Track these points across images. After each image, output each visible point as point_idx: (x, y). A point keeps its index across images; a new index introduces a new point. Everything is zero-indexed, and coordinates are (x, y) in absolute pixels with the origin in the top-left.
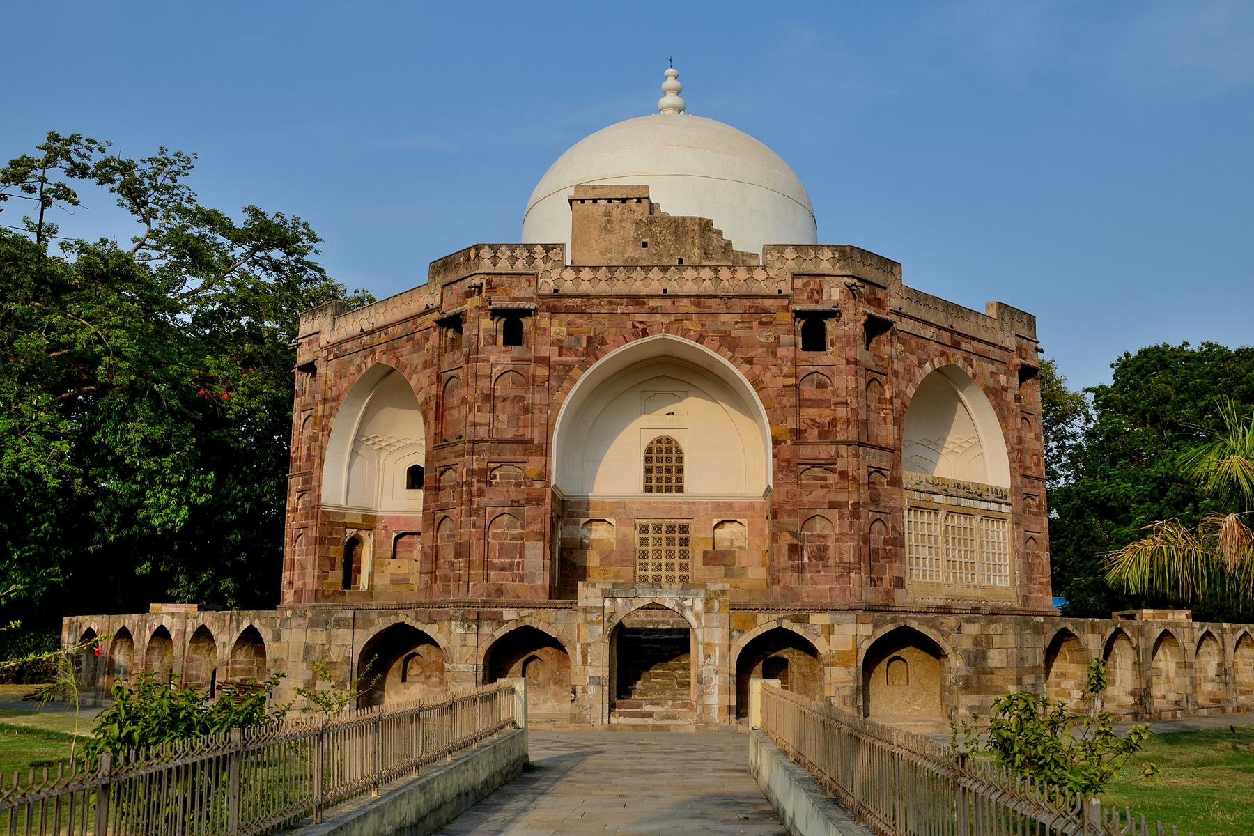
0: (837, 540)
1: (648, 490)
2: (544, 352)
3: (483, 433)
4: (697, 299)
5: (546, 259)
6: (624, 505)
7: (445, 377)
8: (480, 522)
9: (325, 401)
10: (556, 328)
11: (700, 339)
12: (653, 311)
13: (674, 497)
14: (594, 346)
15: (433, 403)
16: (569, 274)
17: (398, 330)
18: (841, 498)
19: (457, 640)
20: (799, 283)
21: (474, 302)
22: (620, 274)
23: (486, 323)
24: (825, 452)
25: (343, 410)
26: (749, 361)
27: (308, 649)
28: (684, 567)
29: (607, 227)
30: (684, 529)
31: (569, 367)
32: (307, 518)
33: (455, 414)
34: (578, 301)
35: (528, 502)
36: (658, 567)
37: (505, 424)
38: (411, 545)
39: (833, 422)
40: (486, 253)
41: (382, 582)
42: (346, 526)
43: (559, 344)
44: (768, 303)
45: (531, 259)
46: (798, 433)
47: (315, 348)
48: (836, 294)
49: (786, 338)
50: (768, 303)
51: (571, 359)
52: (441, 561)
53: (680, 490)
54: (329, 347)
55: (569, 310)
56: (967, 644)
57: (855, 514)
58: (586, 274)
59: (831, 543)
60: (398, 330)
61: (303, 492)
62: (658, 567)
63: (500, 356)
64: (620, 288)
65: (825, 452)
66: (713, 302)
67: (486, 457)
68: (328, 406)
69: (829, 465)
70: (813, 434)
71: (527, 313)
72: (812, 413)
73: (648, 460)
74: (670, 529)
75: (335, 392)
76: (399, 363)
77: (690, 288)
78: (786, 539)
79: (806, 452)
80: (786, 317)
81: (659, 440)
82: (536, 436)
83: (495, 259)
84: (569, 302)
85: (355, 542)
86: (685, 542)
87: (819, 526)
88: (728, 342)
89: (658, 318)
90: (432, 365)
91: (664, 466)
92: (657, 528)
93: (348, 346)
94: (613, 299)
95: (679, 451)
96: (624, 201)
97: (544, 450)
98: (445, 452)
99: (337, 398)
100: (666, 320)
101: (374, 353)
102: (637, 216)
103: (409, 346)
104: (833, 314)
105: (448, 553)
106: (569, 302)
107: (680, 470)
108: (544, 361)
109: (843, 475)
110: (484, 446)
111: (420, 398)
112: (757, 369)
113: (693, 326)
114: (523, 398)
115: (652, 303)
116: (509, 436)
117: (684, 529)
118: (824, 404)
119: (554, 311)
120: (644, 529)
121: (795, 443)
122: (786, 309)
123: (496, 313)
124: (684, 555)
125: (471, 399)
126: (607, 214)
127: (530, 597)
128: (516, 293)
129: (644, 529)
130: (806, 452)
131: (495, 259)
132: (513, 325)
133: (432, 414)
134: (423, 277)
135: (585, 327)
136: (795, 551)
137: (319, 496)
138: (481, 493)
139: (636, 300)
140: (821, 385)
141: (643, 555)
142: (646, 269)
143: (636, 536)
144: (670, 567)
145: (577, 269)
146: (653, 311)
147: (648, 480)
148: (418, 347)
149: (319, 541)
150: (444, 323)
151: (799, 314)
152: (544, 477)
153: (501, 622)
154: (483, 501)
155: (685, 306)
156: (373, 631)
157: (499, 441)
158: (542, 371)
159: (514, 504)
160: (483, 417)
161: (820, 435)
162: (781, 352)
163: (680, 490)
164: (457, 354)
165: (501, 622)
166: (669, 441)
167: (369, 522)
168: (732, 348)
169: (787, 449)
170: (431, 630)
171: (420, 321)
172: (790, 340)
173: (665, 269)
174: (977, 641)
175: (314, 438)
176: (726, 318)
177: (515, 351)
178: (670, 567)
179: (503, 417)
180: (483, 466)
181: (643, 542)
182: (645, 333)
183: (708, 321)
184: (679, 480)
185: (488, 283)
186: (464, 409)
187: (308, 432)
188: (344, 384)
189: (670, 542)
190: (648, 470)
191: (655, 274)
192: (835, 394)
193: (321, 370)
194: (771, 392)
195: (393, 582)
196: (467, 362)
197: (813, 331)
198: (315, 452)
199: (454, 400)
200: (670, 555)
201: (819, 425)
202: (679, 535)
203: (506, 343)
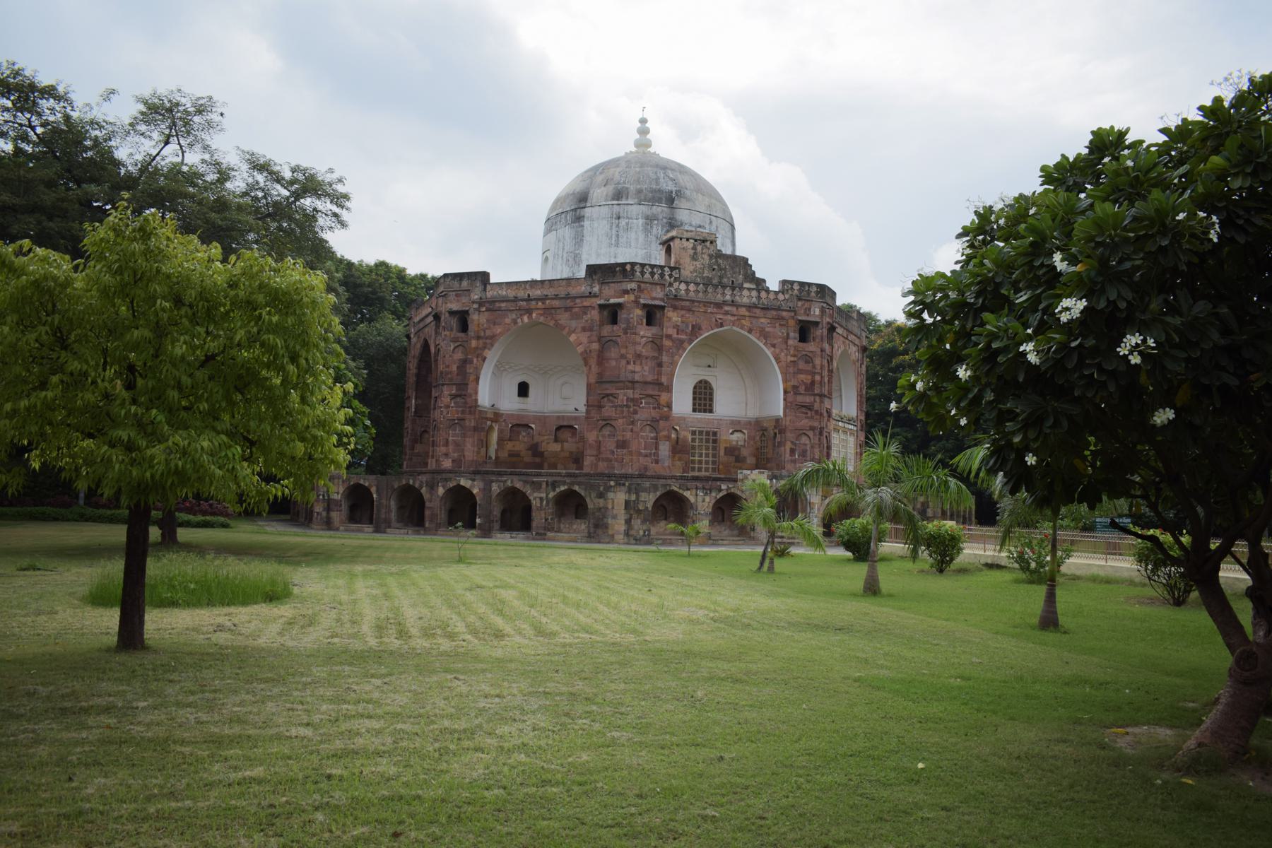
0: (812, 447)
1: (694, 410)
2: (671, 331)
3: (637, 377)
4: (750, 307)
5: (671, 276)
6: (684, 419)
7: (604, 340)
8: (635, 429)
9: (478, 338)
10: (674, 317)
11: (750, 331)
12: (727, 313)
13: (707, 416)
14: (696, 330)
15: (594, 355)
16: (683, 286)
17: (556, 303)
18: (816, 424)
19: (700, 499)
20: (800, 303)
21: (632, 297)
22: (710, 289)
23: (638, 312)
24: (808, 399)
25: (496, 345)
26: (774, 346)
27: (627, 503)
28: (714, 456)
29: (694, 258)
30: (715, 434)
31: (682, 342)
32: (463, 412)
33: (613, 363)
34: (688, 303)
35: (661, 418)
36: (701, 455)
37: (643, 371)
38: (519, 433)
39: (813, 383)
40: (638, 268)
41: (504, 455)
42: (487, 419)
43: (676, 327)
44: (784, 314)
45: (662, 275)
46: (795, 387)
47: (464, 300)
48: (817, 312)
49: (792, 334)
50: (784, 314)
51: (683, 337)
52: (603, 449)
53: (711, 411)
54: (481, 303)
55: (683, 308)
56: (919, 506)
57: (821, 434)
58: (692, 287)
59: (808, 448)
60: (556, 303)
61: (454, 397)
62: (701, 455)
63: (645, 332)
64: (710, 297)
65: (808, 399)
66: (758, 311)
67: (638, 391)
68: (481, 341)
69: (809, 407)
70: (802, 389)
71: (663, 308)
72: (802, 377)
73: (694, 393)
74: (708, 433)
75: (488, 333)
76: (557, 325)
77: (745, 300)
78: (789, 446)
79: (800, 399)
80: (792, 323)
81: (700, 382)
82: (664, 380)
83: (643, 273)
84: (684, 303)
85: (491, 428)
86: (715, 441)
87: (804, 440)
88: (764, 335)
89: (729, 317)
90: (591, 330)
91: (703, 396)
92: (701, 433)
93: (503, 305)
94: (706, 304)
95: (711, 389)
96: (704, 241)
97: (669, 389)
98: (607, 386)
99: (493, 338)
100: (732, 318)
101: (530, 314)
102: (710, 252)
103: (567, 315)
104: (816, 324)
105: (610, 444)
106: (684, 303)
107: (711, 400)
108: (669, 337)
109: (817, 412)
110: (637, 385)
111: (580, 349)
112: (777, 351)
113: (746, 323)
114: (657, 358)
115: (727, 308)
116: (649, 379)
117: (715, 434)
118: (806, 372)
119: (675, 308)
120: (694, 433)
121: (795, 394)
122: (793, 318)
123: (645, 306)
124: (714, 449)
125: (629, 356)
126: (694, 248)
127: (663, 473)
128: (654, 295)
129: (694, 433)
130: (800, 399)
131: (643, 273)
132: (652, 315)
133: (593, 362)
134: (582, 273)
135: (691, 319)
136: (792, 451)
137: (476, 400)
138: (636, 412)
139: (719, 305)
140: (807, 362)
141: (693, 447)
142: (716, 286)
143: (690, 437)
144: (707, 455)
145: (687, 283)
146: (727, 313)
147: (694, 404)
148: (576, 317)
149: (475, 429)
150: (601, 307)
151: (800, 321)
152: (669, 406)
153: (720, 490)
154: (637, 417)
155: (743, 311)
156: (658, 494)
157: (646, 383)
158: (667, 343)
159: (655, 420)
160: (638, 368)
161: (806, 389)
162: (790, 342)
163: (711, 411)
164: (615, 327)
165: (720, 490)
166: (706, 382)
167: (497, 416)
168: (766, 338)
169: (791, 397)
170: (687, 494)
171: (578, 301)
172: (794, 335)
173: (733, 289)
174: (923, 504)
175: (464, 362)
176: (763, 320)
177: (654, 330)
178: (707, 455)
179: (646, 368)
180: (637, 396)
181: (693, 440)
182: (722, 325)
183: (754, 321)
184: (711, 405)
185: (639, 287)
186: (623, 362)
187: (459, 355)
188: (498, 330)
189: (707, 441)
190: (694, 399)
191: (728, 292)
192: (814, 367)
193: (474, 317)
194: (783, 364)
195: (510, 455)
196: (626, 333)
197: (804, 332)
198: (470, 369)
199: (613, 353)
200: (707, 448)
201: (805, 384)
202: (712, 437)
203: (649, 324)
